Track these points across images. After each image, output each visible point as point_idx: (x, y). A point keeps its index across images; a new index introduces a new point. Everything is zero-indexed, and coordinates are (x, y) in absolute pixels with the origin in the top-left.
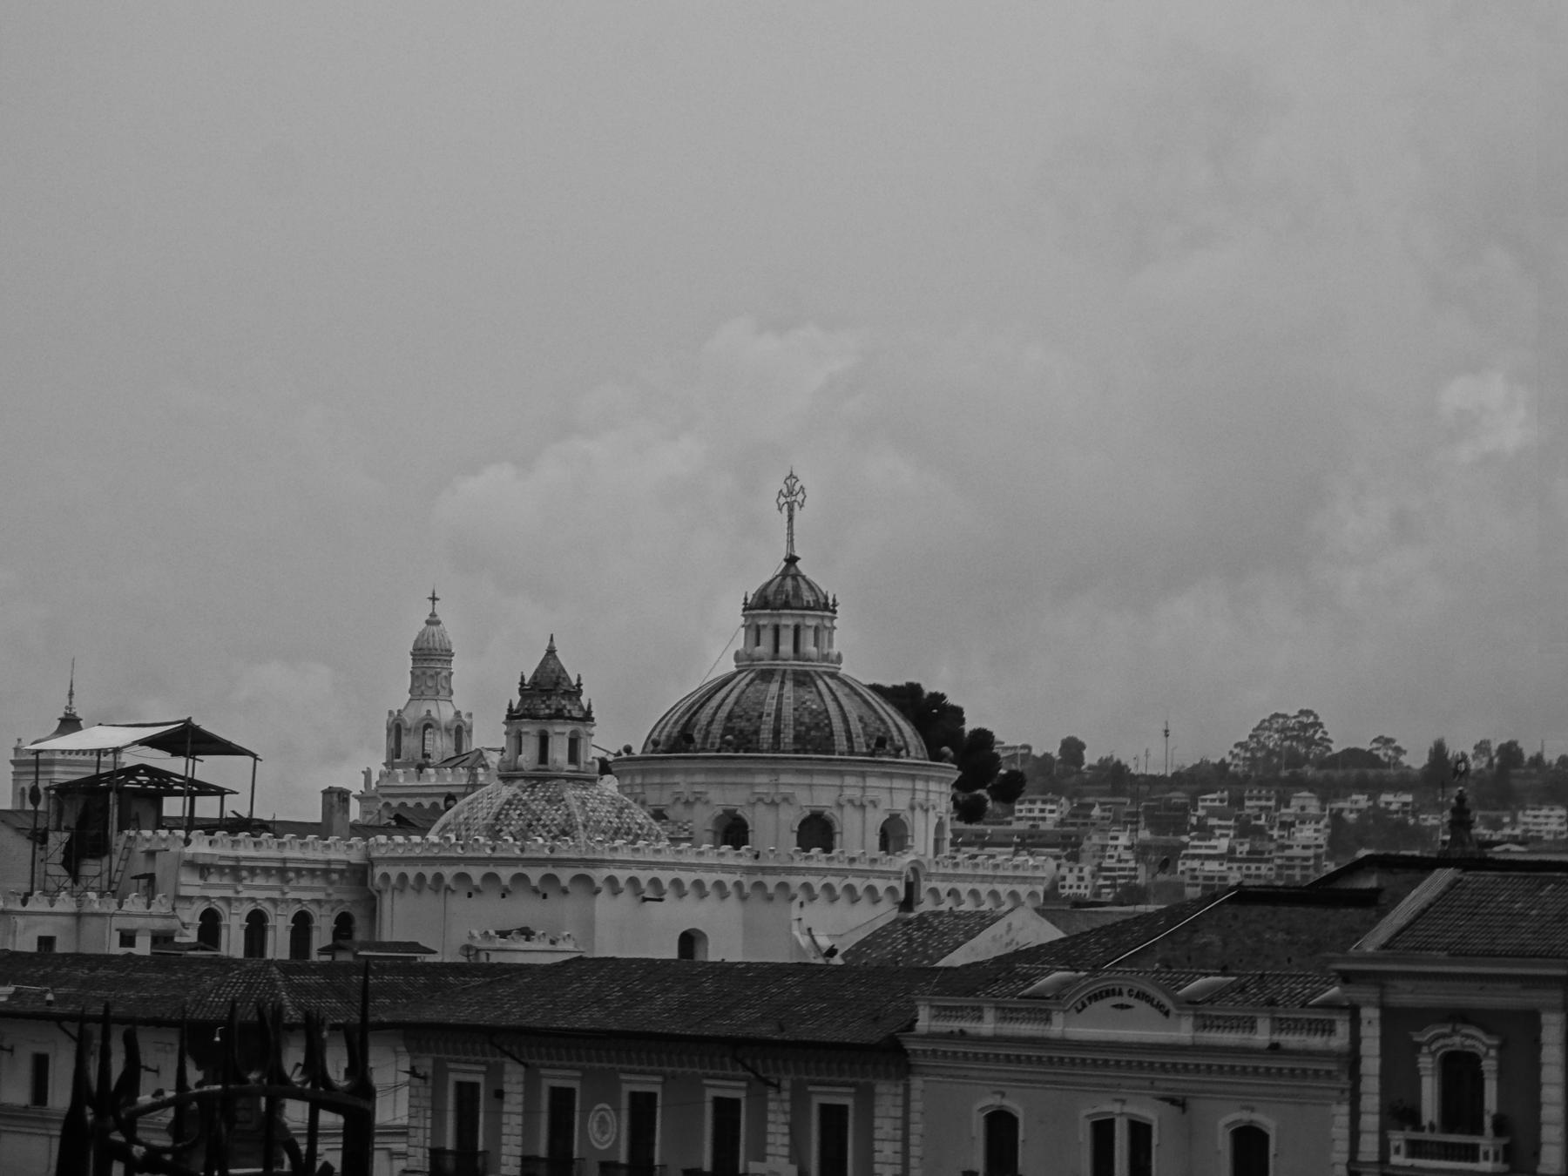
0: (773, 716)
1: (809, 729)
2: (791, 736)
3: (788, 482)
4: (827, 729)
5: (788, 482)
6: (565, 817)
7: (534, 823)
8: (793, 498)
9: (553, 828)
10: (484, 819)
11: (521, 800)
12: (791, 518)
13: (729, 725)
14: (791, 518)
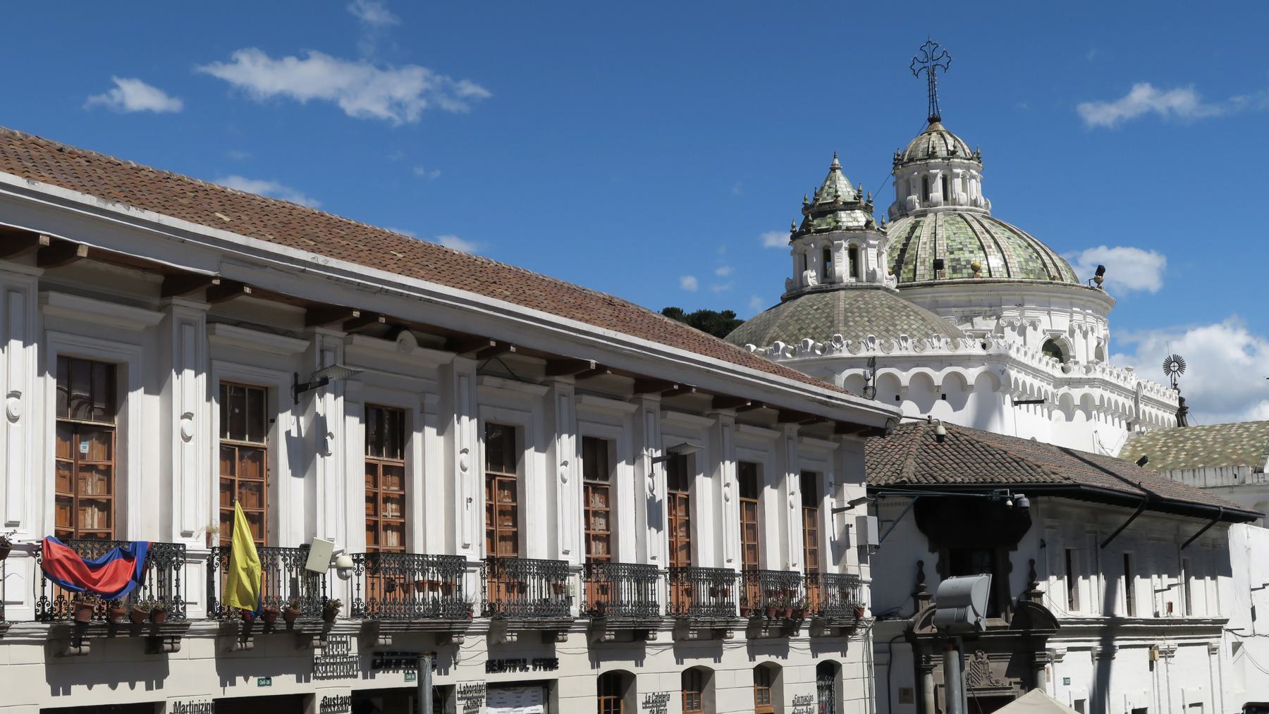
0: (993, 247)
1: (1027, 261)
2: (1017, 266)
3: (925, 48)
4: (1039, 261)
5: (925, 48)
6: (921, 322)
7: (891, 328)
8: (935, 63)
9: (915, 333)
10: (829, 327)
11: (859, 308)
12: (931, 83)
13: (952, 256)
14: (931, 83)
